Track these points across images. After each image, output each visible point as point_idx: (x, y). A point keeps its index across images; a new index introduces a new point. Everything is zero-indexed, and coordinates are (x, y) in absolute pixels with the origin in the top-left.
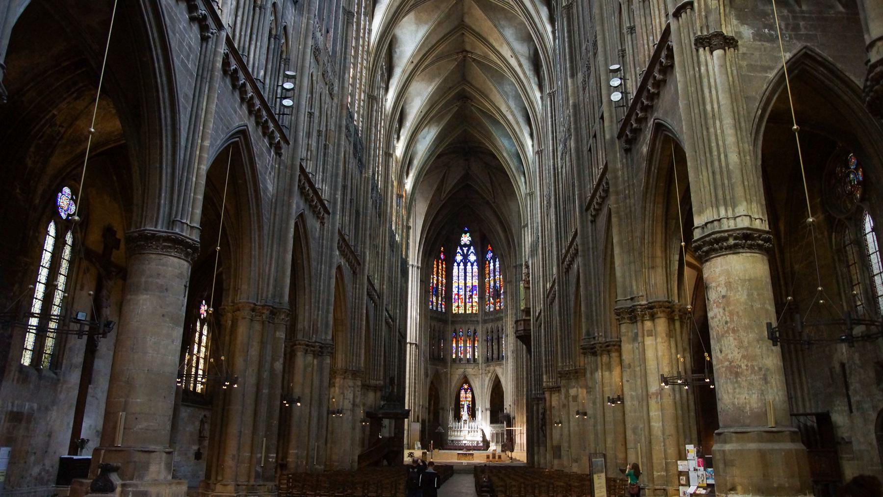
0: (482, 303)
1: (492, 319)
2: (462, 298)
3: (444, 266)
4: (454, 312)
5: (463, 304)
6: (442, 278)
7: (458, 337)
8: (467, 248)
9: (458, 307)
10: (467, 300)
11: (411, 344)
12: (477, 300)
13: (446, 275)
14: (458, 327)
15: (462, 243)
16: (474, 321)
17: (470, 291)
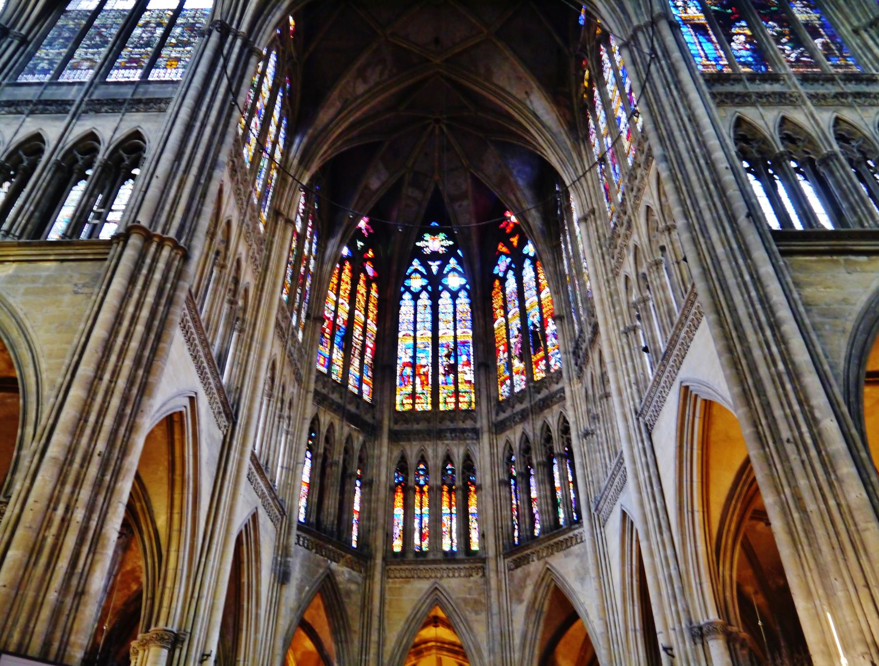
0: (488, 379)
1: (523, 410)
2: (425, 374)
3: (374, 293)
4: (399, 408)
5: (428, 388)
6: (366, 316)
7: (411, 478)
8: (438, 263)
9: (413, 396)
10: (441, 378)
11: (148, 237)
12: (470, 377)
13: (377, 315)
14: (412, 450)
15: (427, 251)
16: (464, 431)
17: (448, 356)
